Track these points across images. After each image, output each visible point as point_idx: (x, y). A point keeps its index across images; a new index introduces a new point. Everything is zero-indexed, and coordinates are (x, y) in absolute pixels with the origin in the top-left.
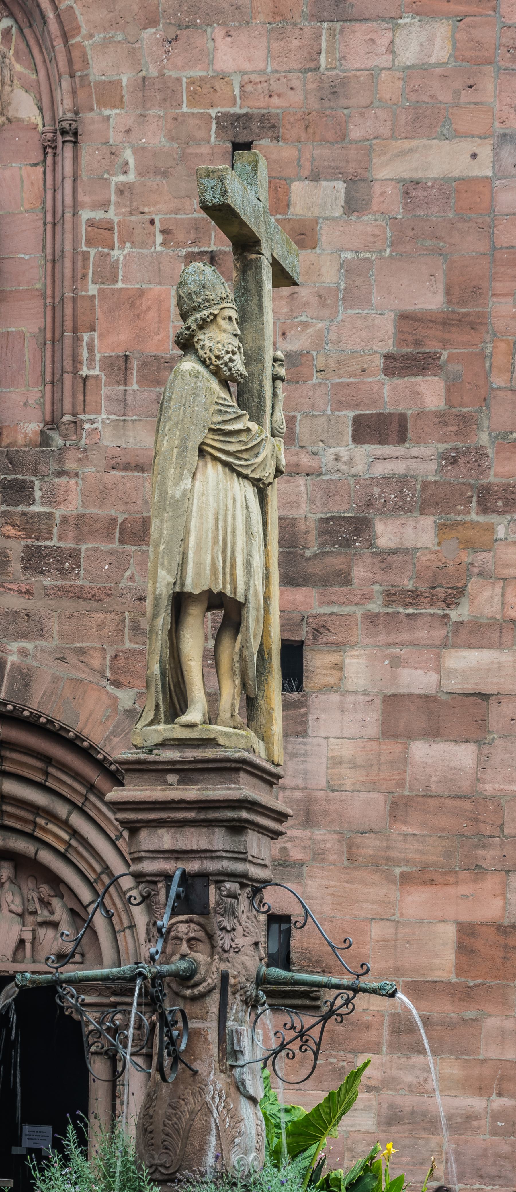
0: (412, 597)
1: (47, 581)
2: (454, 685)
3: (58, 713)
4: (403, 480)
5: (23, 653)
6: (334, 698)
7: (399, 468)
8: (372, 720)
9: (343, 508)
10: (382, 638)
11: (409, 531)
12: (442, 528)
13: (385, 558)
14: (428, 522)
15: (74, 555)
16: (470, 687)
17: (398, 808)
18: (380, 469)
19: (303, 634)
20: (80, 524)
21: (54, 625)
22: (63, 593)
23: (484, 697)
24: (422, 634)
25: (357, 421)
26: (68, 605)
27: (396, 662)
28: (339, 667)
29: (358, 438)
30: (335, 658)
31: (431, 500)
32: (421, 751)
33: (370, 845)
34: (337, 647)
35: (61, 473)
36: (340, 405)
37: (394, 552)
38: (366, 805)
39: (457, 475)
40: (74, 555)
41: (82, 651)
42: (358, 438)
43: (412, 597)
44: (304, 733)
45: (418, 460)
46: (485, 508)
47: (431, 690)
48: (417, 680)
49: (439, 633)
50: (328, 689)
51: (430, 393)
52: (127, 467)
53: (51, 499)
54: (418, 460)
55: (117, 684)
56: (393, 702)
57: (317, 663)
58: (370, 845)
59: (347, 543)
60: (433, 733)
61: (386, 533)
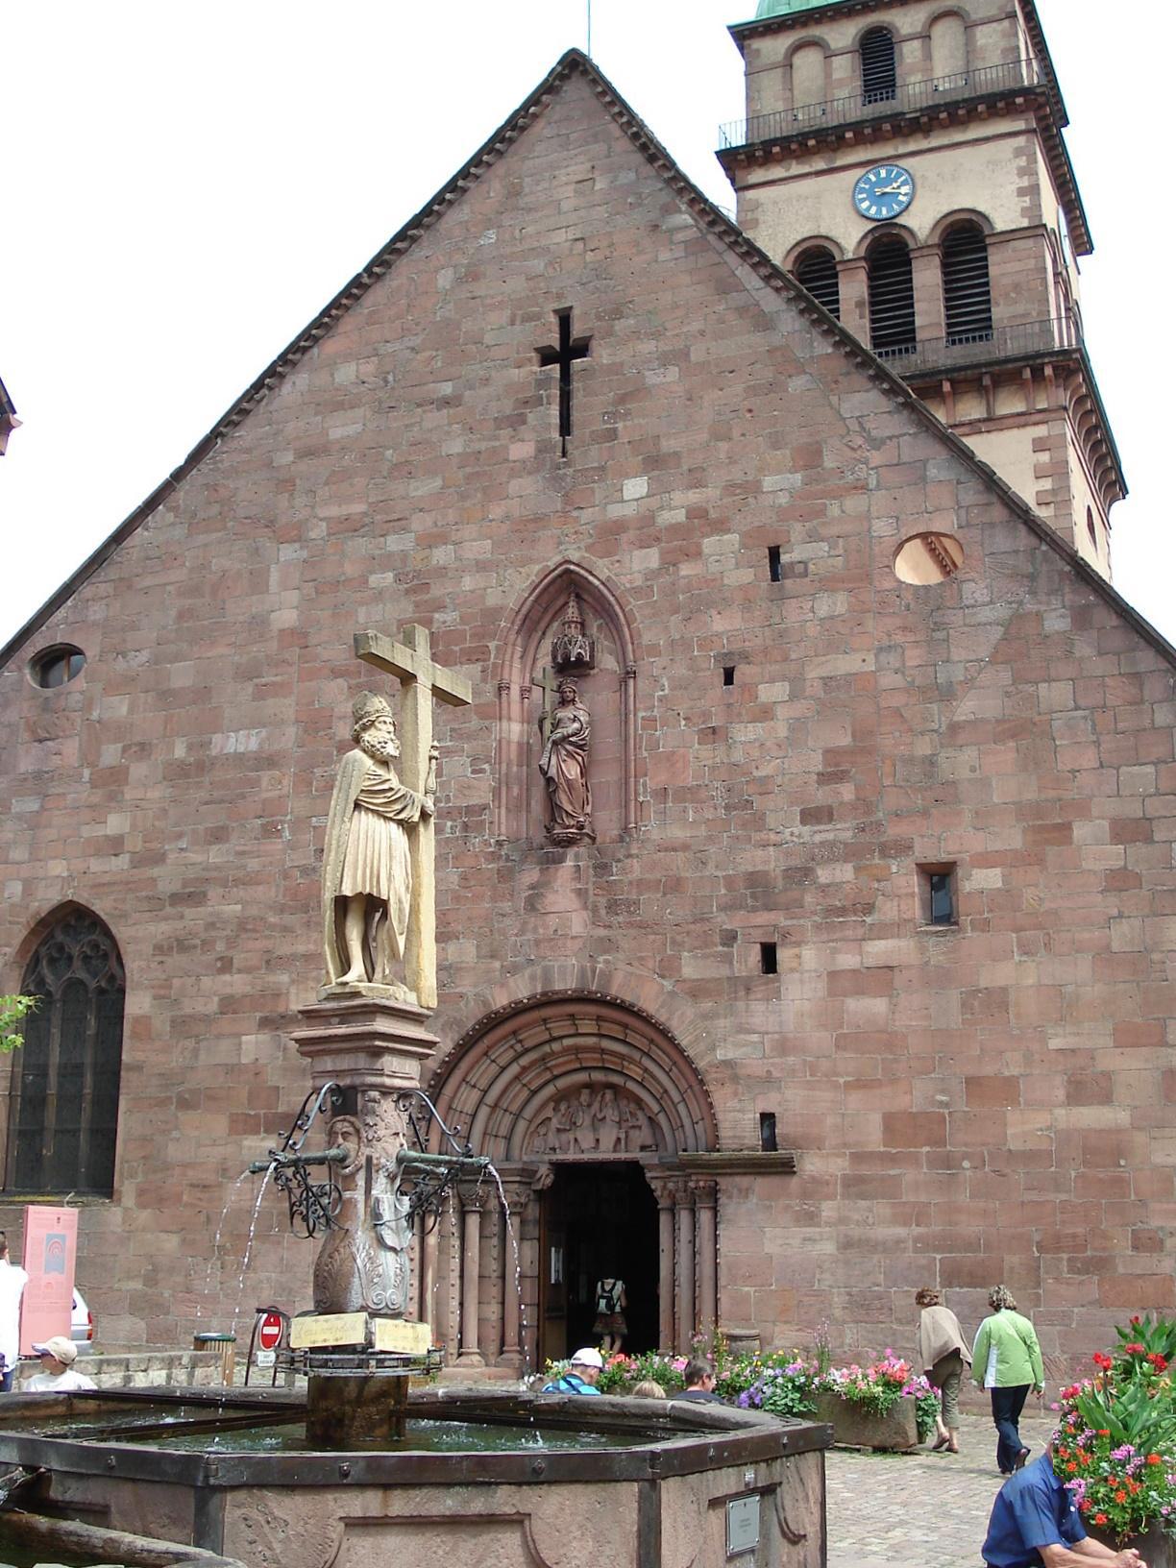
0: (842, 911)
1: (621, 919)
2: (870, 962)
3: (629, 998)
4: (832, 844)
5: (607, 962)
6: (796, 976)
7: (830, 836)
8: (821, 987)
9: (796, 862)
10: (825, 937)
11: (838, 872)
12: (857, 869)
13: (824, 889)
14: (849, 867)
15: (636, 903)
16: (881, 963)
17: (842, 1042)
18: (818, 838)
19: (776, 939)
20: (640, 884)
21: (624, 944)
22: (631, 924)
23: (890, 968)
24: (849, 933)
25: (803, 812)
26: (633, 932)
27: (835, 951)
28: (798, 956)
29: (803, 822)
30: (796, 951)
31: (851, 853)
32: (852, 1004)
33: (825, 1065)
34: (798, 944)
35: (629, 856)
36: (792, 804)
37: (828, 885)
38: (820, 1039)
39: (865, 838)
40: (636, 903)
41: (642, 958)
42: (803, 822)
43: (842, 911)
44: (779, 998)
45: (842, 831)
46: (884, 855)
47: (857, 966)
48: (848, 961)
49: (860, 932)
50: (792, 970)
51: (847, 792)
52: (666, 850)
53: (624, 871)
54: (842, 831)
55: (663, 977)
56: (833, 975)
57: (783, 955)
58: (825, 1065)
59: (800, 883)
60: (860, 992)
61: (823, 875)
